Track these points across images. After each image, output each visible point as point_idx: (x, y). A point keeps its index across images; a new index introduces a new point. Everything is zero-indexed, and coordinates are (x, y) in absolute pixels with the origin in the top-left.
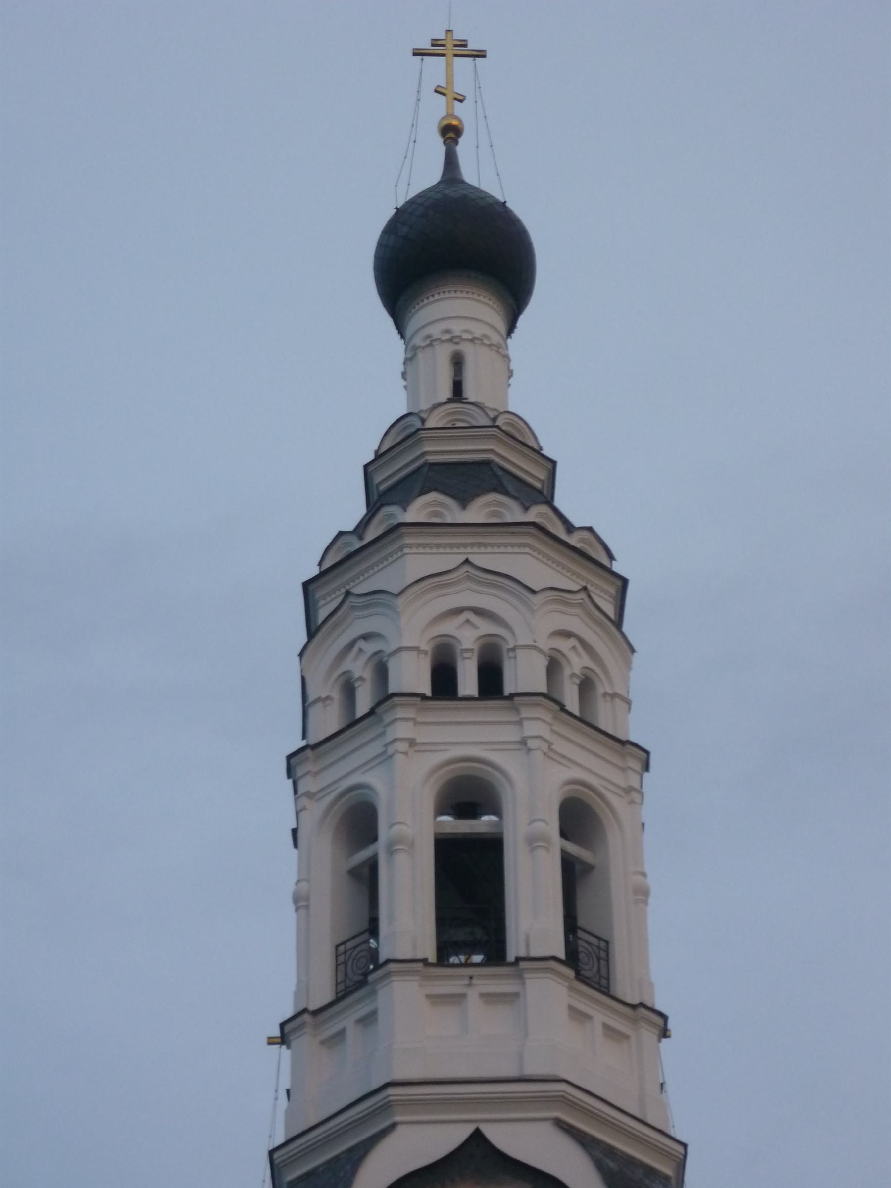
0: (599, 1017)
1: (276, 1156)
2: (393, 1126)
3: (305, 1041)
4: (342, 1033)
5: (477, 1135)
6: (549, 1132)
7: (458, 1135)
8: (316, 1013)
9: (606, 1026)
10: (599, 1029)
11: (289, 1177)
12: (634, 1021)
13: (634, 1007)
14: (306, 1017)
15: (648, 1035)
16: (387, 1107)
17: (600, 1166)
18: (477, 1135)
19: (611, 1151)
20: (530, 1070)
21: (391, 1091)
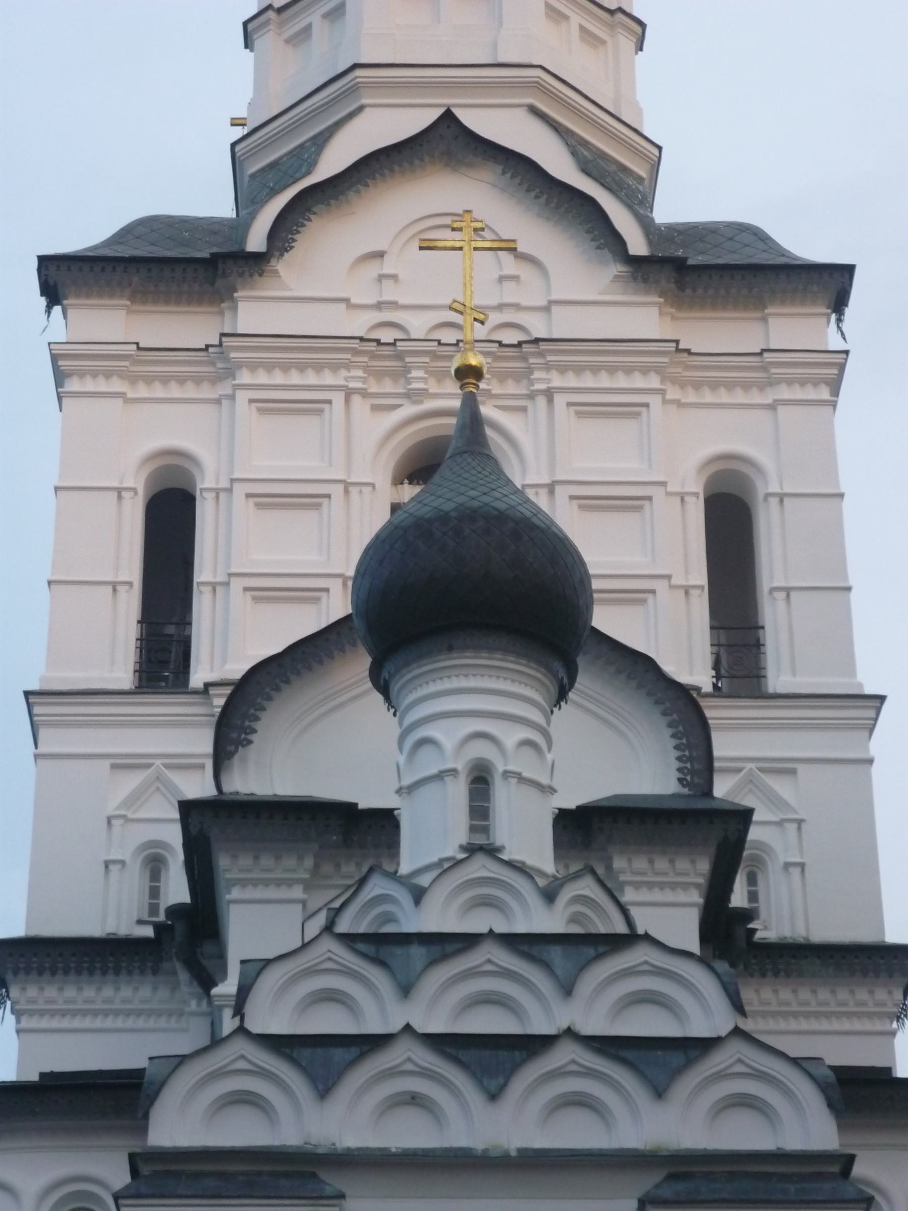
0: (576, 19)
1: (237, 148)
2: (361, 108)
3: (267, 40)
4: (308, 29)
5: (448, 117)
6: (522, 115)
7: (426, 118)
8: (280, 10)
9: (582, 28)
10: (575, 32)
11: (253, 169)
12: (611, 27)
13: (611, 12)
14: (271, 14)
15: (626, 43)
16: (354, 90)
17: (574, 154)
18: (448, 117)
19: (585, 143)
20: (501, 60)
21: (358, 72)
